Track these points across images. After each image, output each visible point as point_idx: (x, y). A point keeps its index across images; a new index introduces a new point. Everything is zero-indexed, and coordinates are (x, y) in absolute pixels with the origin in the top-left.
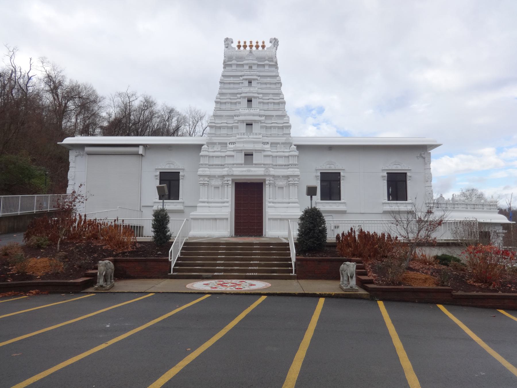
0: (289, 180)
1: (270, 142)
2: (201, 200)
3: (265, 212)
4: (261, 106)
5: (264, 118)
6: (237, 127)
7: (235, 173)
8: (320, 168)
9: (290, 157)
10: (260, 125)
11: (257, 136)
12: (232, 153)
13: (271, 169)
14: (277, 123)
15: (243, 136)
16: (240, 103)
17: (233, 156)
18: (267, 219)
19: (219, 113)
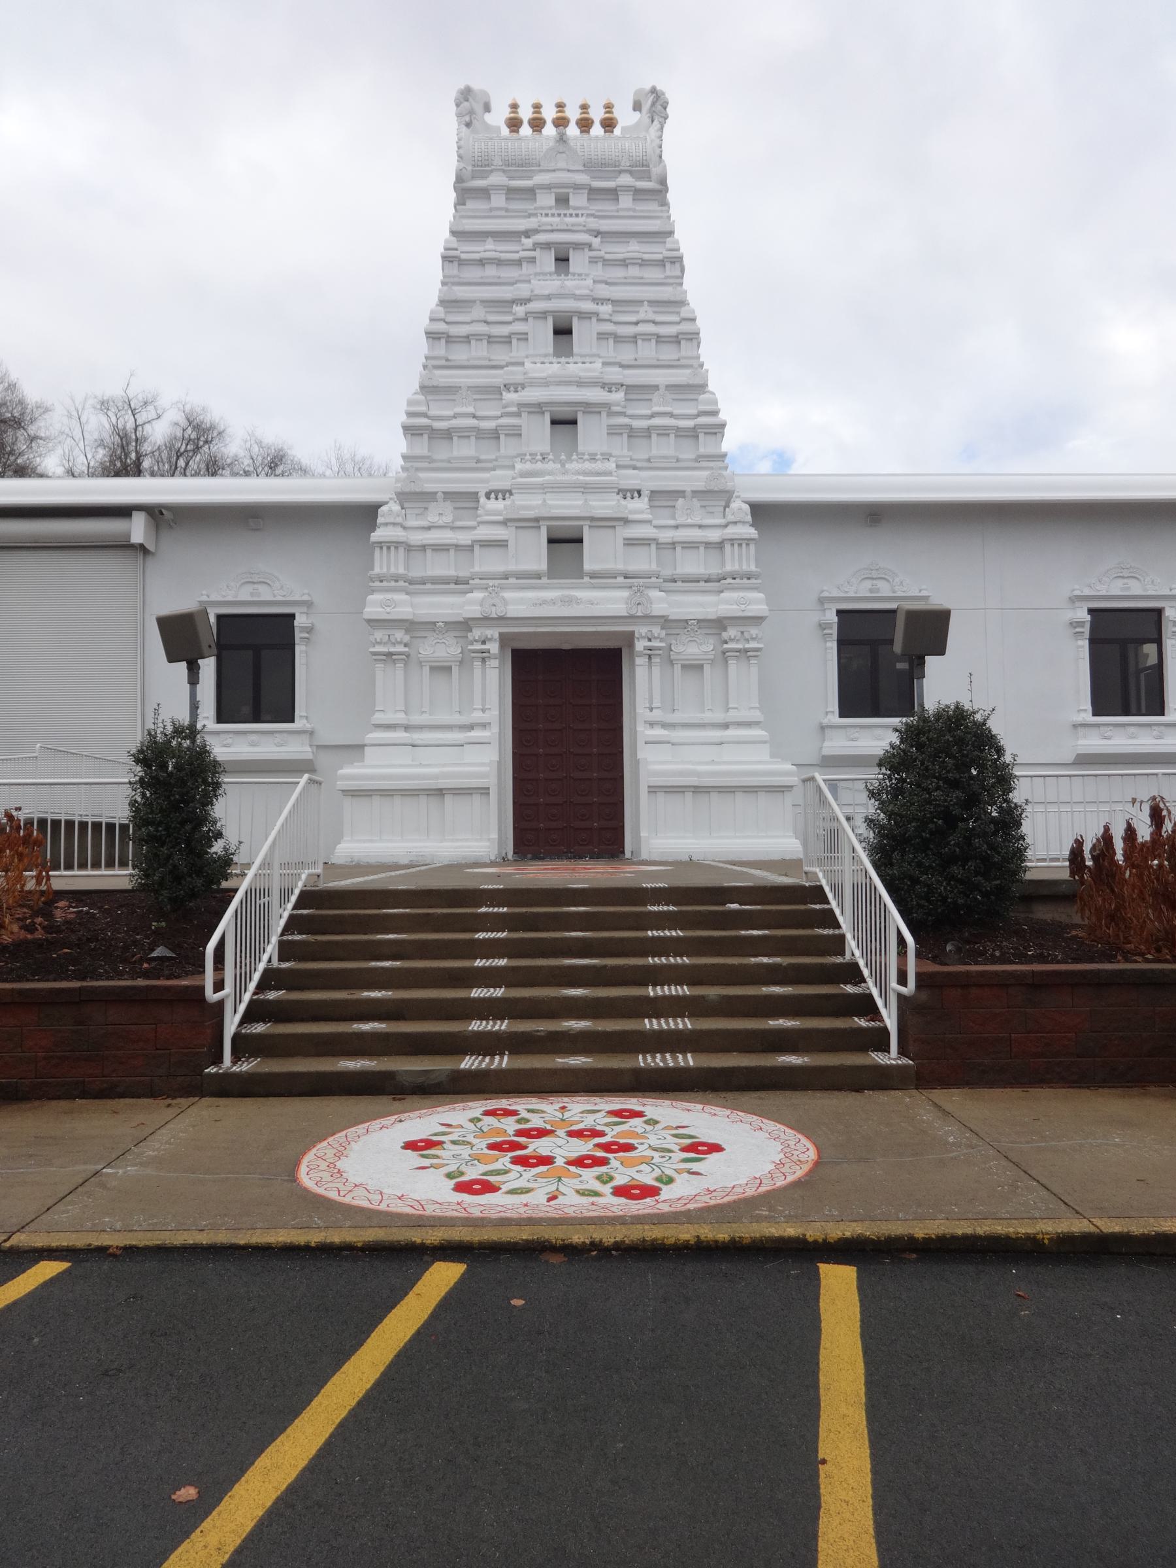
0: (725, 635)
1: (647, 486)
2: (379, 718)
3: (637, 762)
4: (609, 350)
5: (619, 396)
6: (516, 433)
7: (513, 611)
8: (835, 593)
9: (728, 547)
10: (605, 420)
11: (598, 466)
12: (500, 533)
13: (655, 594)
14: (671, 415)
15: (539, 465)
16: (523, 337)
17: (502, 544)
19: (444, 377)
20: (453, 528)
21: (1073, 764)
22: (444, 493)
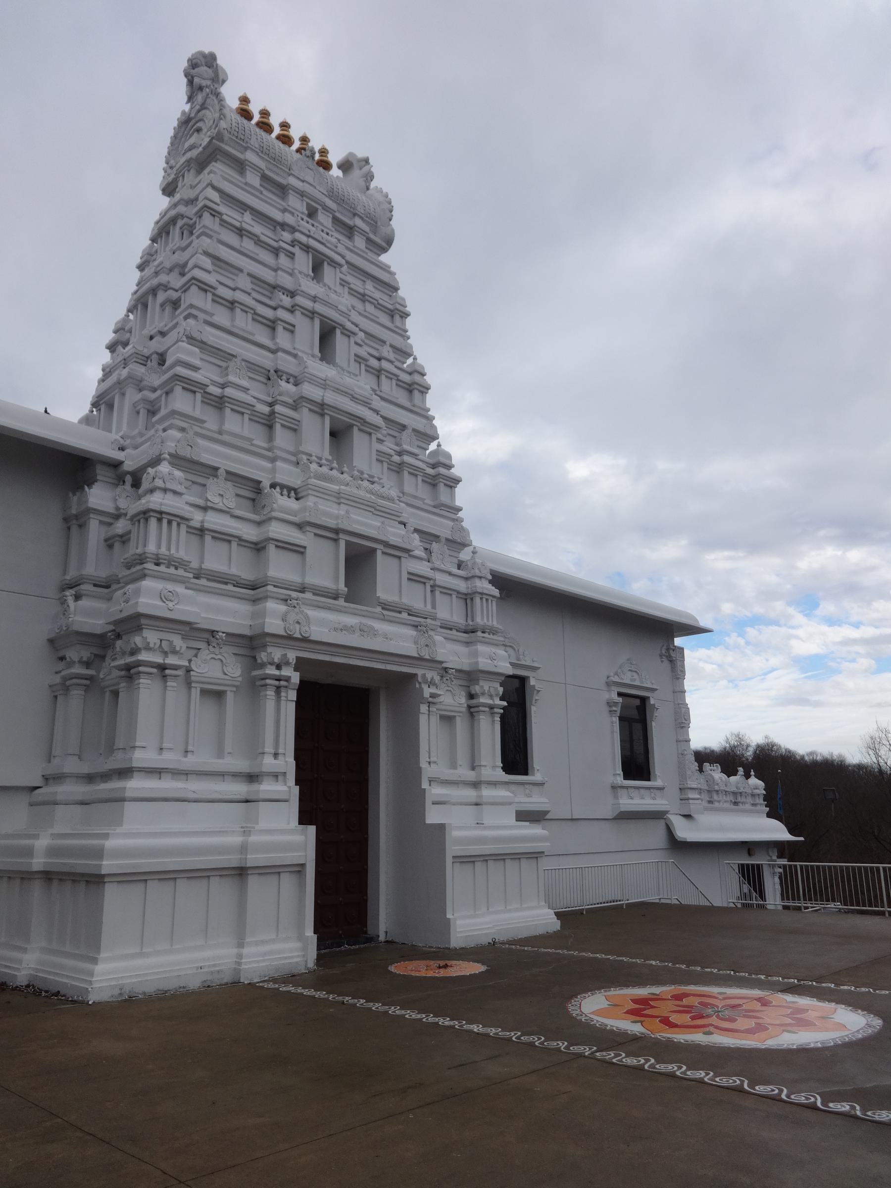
9: (477, 600)
16: (291, 329)
17: (299, 550)
18: (449, 860)
20: (234, 516)
21: (615, 819)
22: (228, 473)
